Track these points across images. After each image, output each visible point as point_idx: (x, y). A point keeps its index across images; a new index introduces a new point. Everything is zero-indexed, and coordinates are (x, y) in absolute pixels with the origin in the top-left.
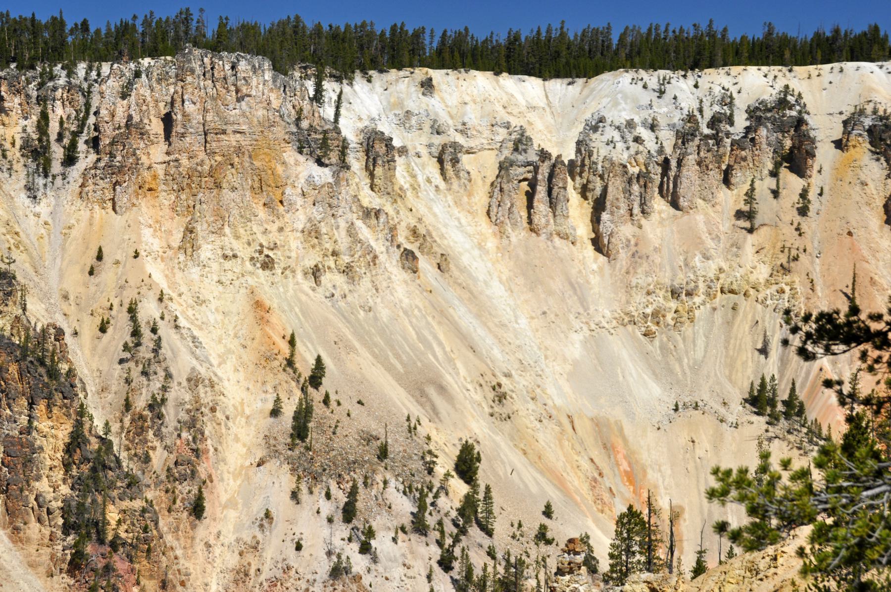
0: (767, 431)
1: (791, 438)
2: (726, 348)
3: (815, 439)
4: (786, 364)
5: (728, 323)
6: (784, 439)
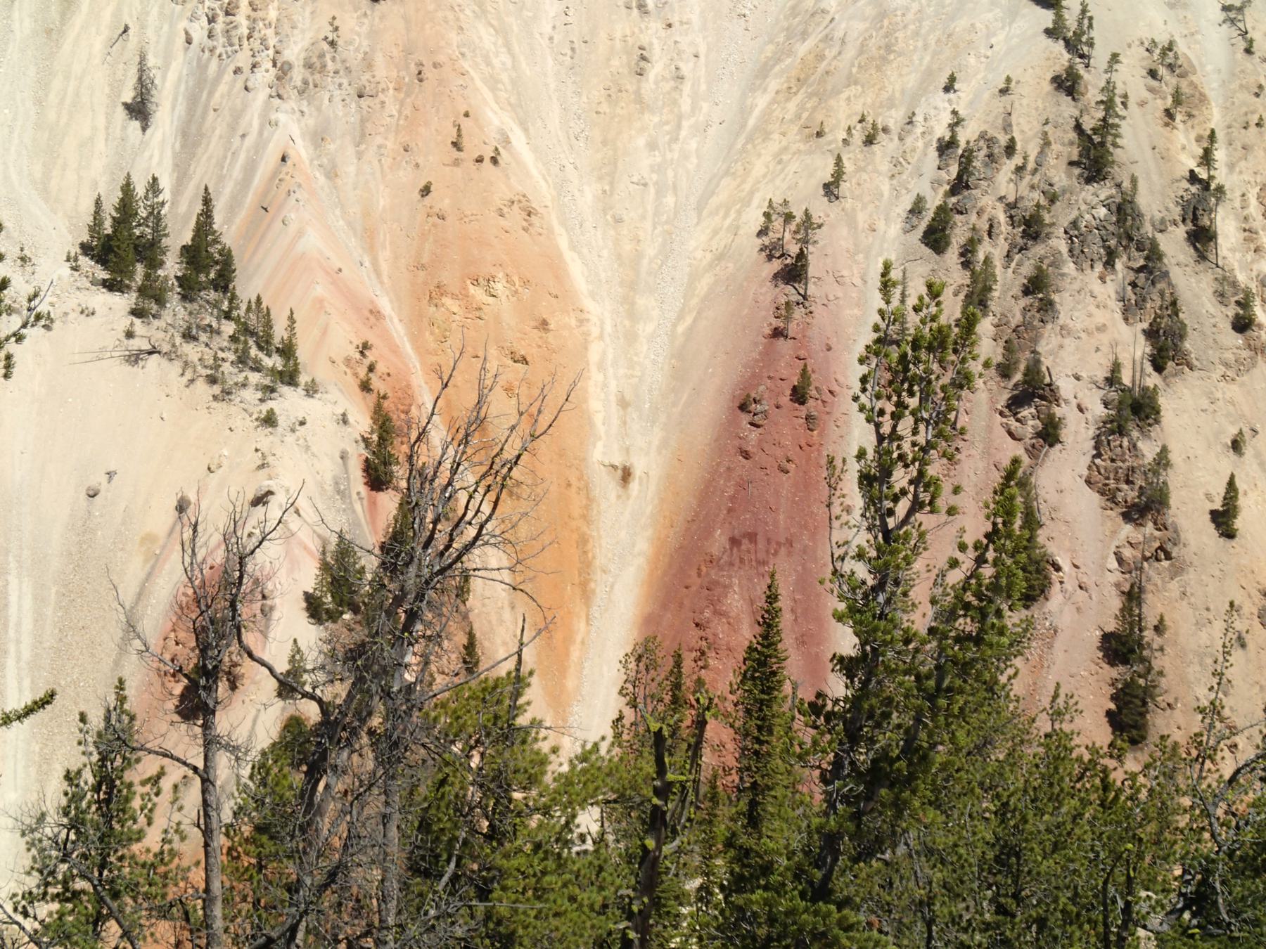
0: (130, 335)
1: (192, 351)
2: (39, 102)
3: (254, 351)
4: (196, 145)
5: (49, 32)
6: (170, 356)
